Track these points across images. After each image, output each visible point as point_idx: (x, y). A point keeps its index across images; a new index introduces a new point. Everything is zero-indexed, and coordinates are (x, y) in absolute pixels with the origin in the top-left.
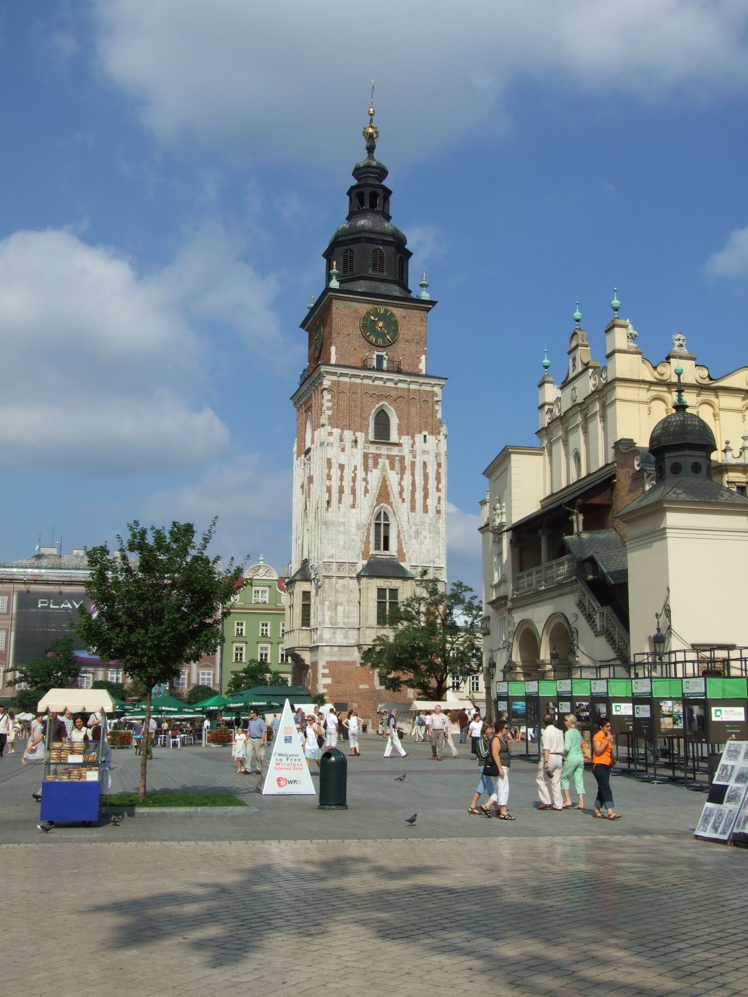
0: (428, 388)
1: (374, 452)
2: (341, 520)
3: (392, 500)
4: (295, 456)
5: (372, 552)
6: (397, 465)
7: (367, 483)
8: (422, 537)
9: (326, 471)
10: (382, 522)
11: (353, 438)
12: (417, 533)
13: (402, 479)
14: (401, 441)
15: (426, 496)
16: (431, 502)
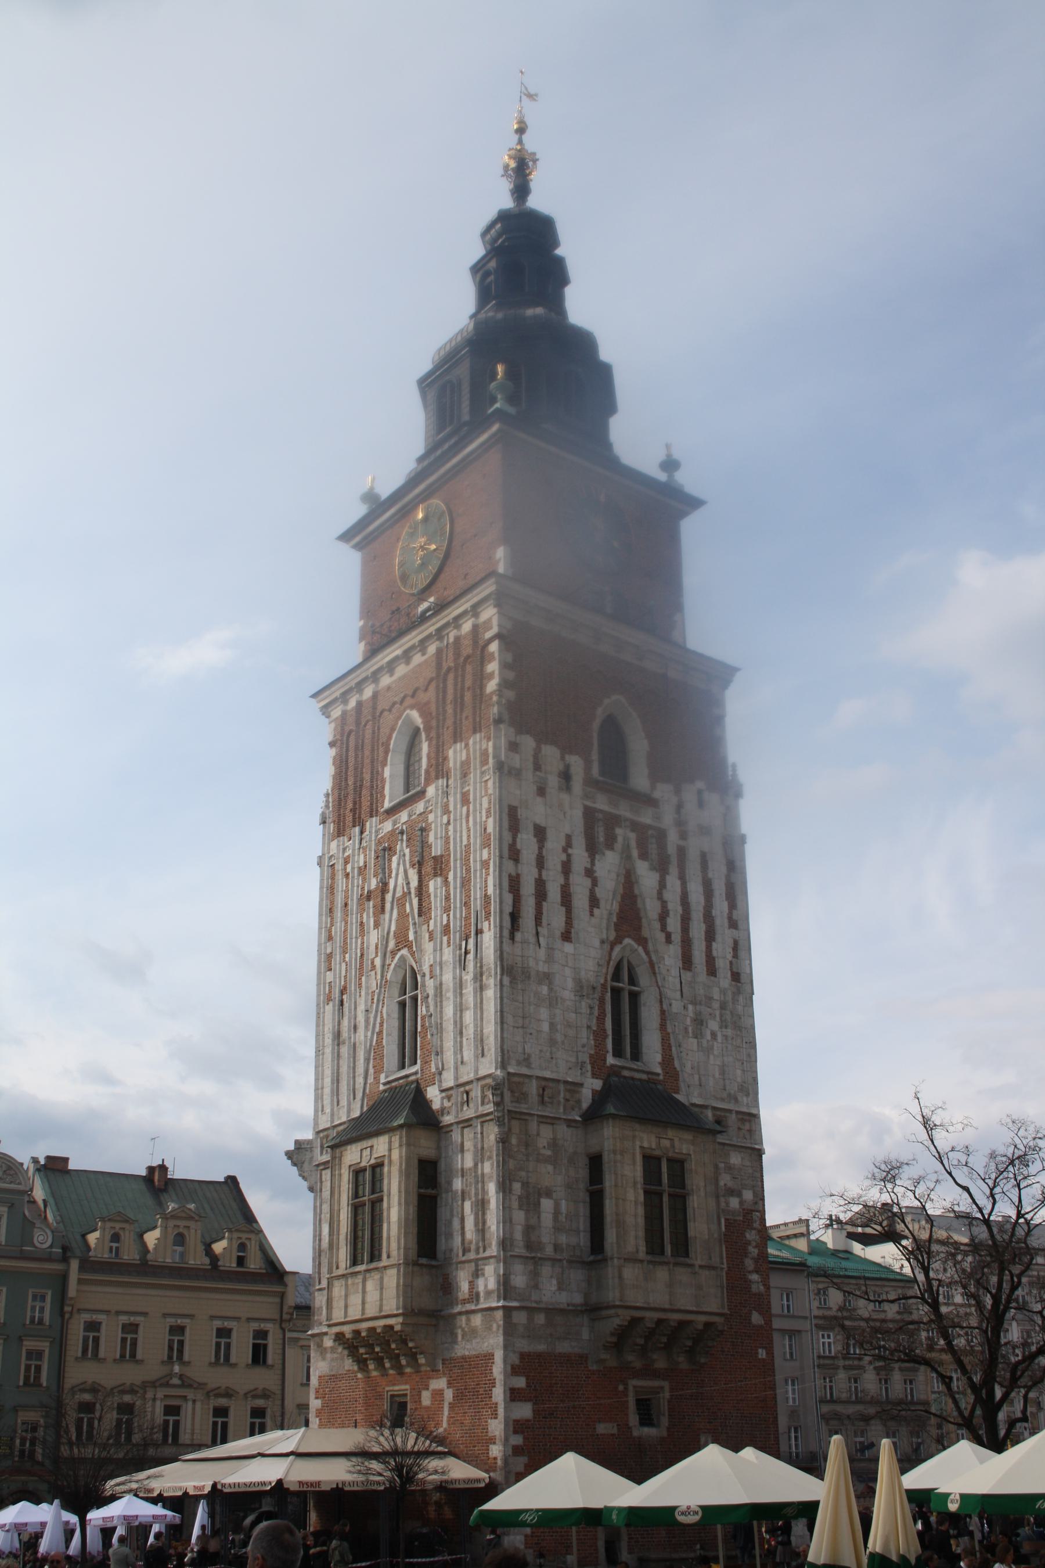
1: (605, 807)
2: (543, 968)
3: (645, 933)
5: (610, 1060)
7: (595, 882)
8: (709, 1038)
9: (508, 837)
10: (624, 985)
11: (561, 767)
12: (699, 1022)
13: (662, 885)
14: (657, 794)
15: (710, 936)
16: (722, 949)
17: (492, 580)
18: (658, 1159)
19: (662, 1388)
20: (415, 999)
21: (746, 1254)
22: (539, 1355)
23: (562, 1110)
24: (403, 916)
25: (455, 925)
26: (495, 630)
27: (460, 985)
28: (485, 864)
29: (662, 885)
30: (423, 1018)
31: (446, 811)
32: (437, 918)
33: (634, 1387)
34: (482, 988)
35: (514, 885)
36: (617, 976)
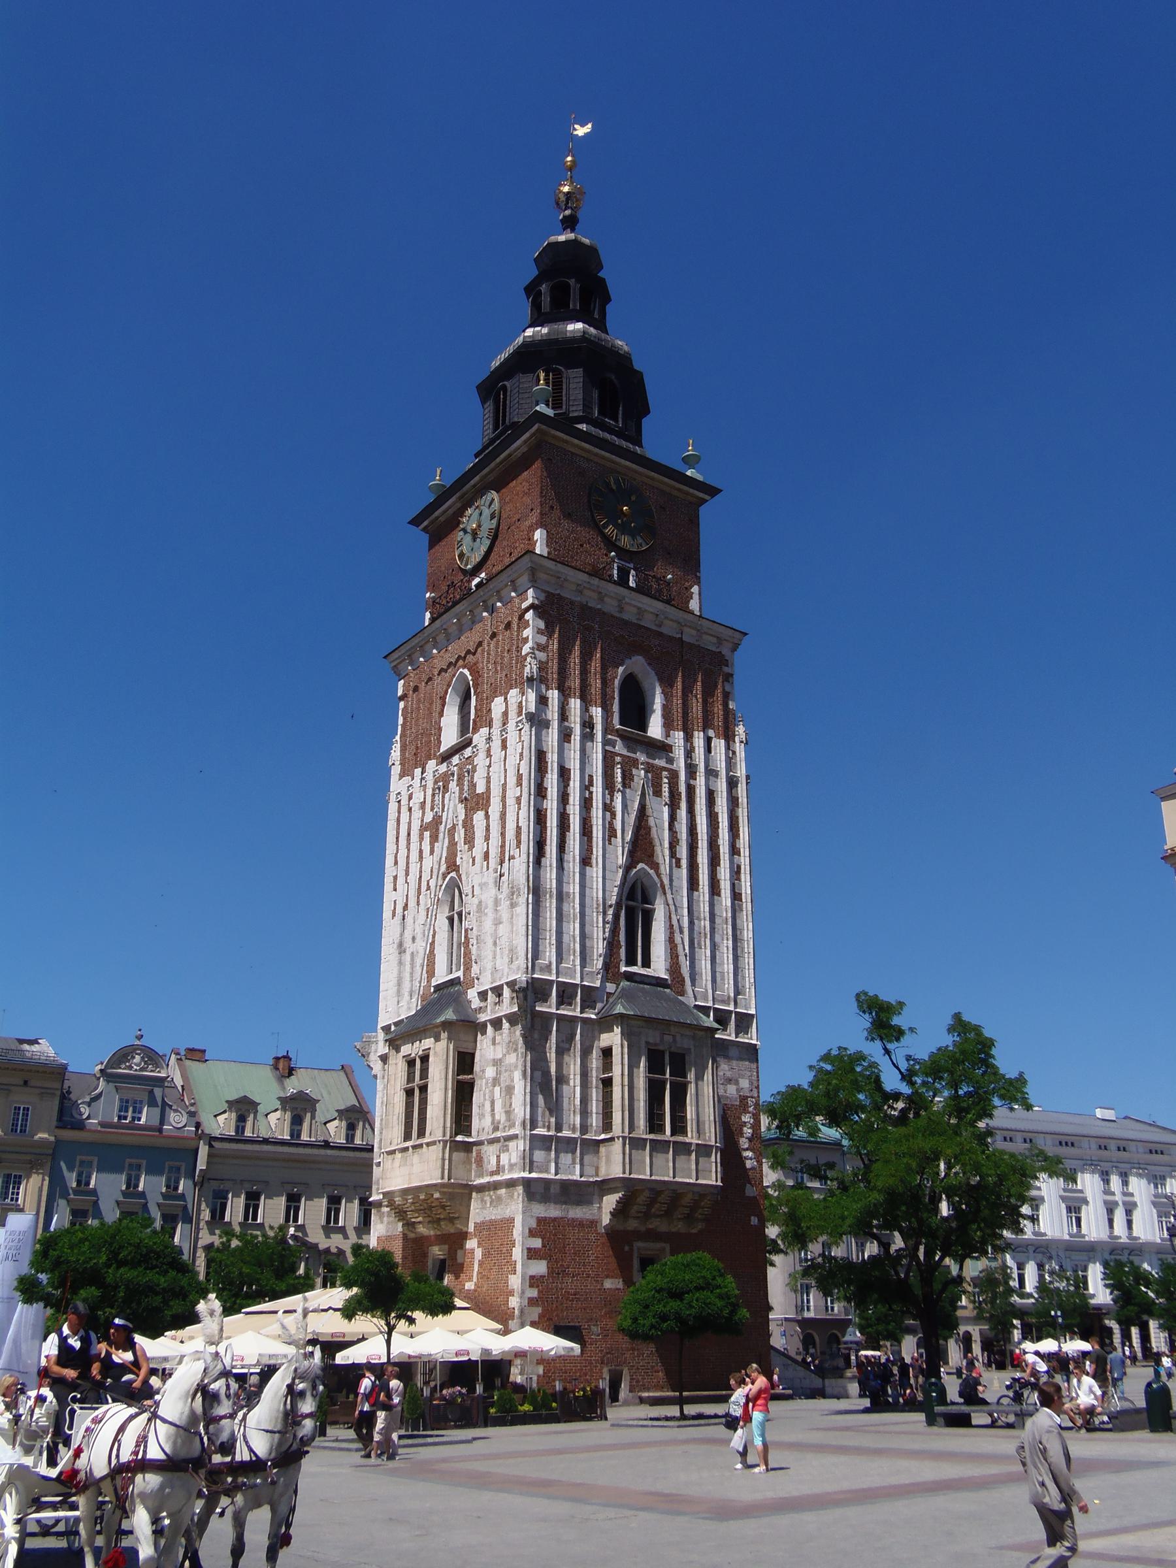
0: (714, 649)
1: (625, 752)
4: (396, 770)
6: (665, 789)
7: (613, 815)
13: (673, 818)
14: (669, 741)
15: (714, 861)
17: (527, 558)
18: (663, 1052)
19: (664, 1249)
20: (460, 914)
21: (741, 1134)
22: (555, 1219)
23: (579, 1009)
24: (453, 844)
25: (494, 853)
26: (530, 601)
27: (497, 902)
28: (518, 800)
29: (673, 818)
30: (466, 931)
31: (489, 755)
32: (479, 846)
33: (639, 1249)
34: (513, 905)
35: (540, 818)
36: (631, 895)
